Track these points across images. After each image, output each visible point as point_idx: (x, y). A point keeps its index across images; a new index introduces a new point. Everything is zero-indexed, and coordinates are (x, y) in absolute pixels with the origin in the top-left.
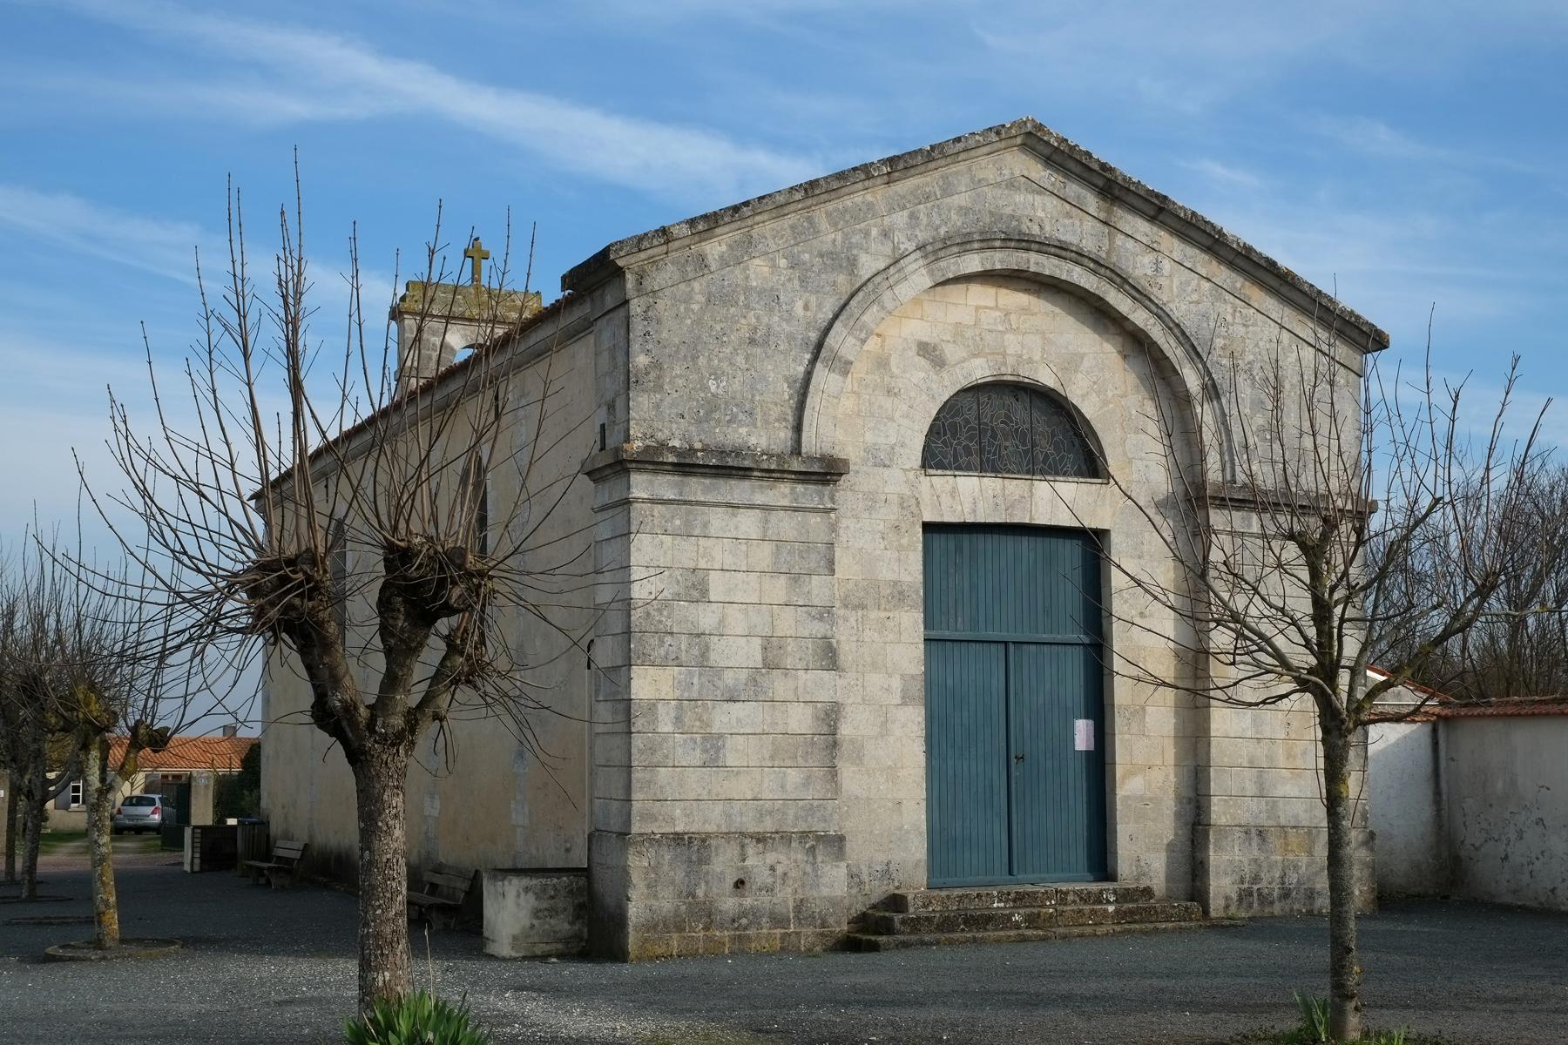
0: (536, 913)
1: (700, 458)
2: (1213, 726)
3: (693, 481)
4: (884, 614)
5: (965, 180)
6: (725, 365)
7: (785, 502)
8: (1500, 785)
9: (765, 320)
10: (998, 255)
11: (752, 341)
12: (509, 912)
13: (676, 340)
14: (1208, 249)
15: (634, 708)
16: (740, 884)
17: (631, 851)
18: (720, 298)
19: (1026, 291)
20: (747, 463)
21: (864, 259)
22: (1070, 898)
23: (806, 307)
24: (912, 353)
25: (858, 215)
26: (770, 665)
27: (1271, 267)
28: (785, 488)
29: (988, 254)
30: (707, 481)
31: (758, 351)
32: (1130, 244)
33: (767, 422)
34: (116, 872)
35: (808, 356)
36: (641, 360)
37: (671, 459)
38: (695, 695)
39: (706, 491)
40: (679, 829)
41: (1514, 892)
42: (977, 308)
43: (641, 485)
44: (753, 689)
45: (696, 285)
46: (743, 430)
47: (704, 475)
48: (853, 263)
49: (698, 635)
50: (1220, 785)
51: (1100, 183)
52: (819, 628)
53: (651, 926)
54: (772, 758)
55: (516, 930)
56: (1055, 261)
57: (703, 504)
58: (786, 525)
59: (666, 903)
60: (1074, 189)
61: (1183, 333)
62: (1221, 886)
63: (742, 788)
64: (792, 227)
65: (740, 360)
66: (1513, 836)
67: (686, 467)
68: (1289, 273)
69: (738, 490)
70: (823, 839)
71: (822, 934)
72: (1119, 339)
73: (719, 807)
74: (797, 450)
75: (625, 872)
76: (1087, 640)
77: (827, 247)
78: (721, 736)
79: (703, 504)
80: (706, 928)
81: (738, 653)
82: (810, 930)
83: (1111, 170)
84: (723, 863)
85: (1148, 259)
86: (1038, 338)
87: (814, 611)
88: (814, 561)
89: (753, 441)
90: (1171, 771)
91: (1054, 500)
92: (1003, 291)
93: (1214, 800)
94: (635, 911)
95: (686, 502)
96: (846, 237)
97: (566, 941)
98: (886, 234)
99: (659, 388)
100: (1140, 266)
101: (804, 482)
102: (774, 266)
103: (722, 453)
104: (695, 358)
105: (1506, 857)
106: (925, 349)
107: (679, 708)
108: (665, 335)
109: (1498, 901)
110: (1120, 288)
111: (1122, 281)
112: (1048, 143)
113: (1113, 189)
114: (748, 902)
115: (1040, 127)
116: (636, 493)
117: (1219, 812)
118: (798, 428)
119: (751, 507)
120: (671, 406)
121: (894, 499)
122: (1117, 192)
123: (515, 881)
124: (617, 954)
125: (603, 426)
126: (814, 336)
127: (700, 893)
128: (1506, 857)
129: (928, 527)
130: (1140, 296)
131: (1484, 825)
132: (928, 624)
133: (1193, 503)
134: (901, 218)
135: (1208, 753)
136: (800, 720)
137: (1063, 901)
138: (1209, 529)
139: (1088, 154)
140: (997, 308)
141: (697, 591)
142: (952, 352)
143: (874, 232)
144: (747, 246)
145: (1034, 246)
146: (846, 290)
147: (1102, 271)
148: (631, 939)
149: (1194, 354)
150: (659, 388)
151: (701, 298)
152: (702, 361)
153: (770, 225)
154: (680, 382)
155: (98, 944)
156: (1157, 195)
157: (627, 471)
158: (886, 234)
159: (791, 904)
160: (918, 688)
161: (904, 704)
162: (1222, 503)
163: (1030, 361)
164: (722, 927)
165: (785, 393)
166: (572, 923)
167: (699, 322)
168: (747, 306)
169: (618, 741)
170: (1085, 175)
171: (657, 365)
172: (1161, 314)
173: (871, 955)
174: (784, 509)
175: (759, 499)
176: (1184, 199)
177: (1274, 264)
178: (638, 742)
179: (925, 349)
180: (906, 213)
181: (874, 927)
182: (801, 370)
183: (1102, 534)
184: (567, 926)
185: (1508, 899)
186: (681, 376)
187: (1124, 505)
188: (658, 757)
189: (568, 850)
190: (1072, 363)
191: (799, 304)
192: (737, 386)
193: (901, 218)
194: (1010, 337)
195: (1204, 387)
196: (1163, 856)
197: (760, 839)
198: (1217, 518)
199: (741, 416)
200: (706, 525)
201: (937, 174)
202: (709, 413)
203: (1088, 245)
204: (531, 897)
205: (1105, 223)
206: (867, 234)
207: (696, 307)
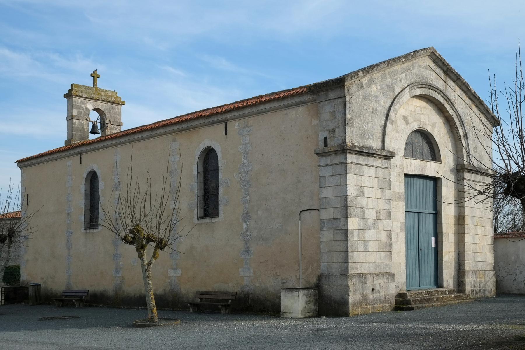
0: (306, 303)
1: (364, 150)
2: (466, 239)
3: (361, 157)
4: (397, 203)
5: (417, 65)
6: (367, 119)
7: (380, 165)
8: (513, 258)
9: (375, 106)
10: (424, 89)
11: (373, 112)
12: (296, 304)
13: (356, 111)
14: (465, 92)
15: (349, 232)
16: (373, 290)
17: (349, 279)
18: (366, 97)
19: (425, 101)
20: (374, 152)
21: (396, 88)
22: (440, 293)
23: (384, 102)
24: (402, 119)
25: (395, 73)
26: (378, 218)
27: (478, 99)
28: (380, 160)
29: (422, 89)
30: (364, 157)
31: (374, 115)
32: (450, 89)
33: (376, 139)
34: (155, 295)
35: (385, 118)
36: (348, 116)
37: (358, 150)
38: (362, 228)
39: (364, 160)
40: (359, 272)
41: (518, 290)
42: (415, 106)
43: (351, 158)
44: (374, 227)
45: (360, 93)
46: (371, 141)
47: (363, 155)
48: (394, 88)
49: (362, 208)
50: (468, 257)
51: (445, 69)
52: (387, 207)
53: (354, 305)
54: (378, 248)
55: (302, 309)
56: (435, 93)
57: (363, 165)
58: (381, 172)
59: (358, 297)
60: (439, 71)
61: (460, 118)
62: (468, 288)
63: (372, 258)
64: (381, 76)
65: (370, 118)
66: (518, 273)
67: (360, 153)
68: (482, 101)
69: (370, 161)
70: (390, 275)
71: (390, 306)
72: (443, 118)
73: (367, 265)
74: (383, 148)
75: (348, 286)
76: (434, 212)
77: (388, 83)
78: (367, 241)
79: (363, 165)
80: (366, 305)
81: (371, 214)
82: (387, 305)
83: (449, 65)
84: (369, 285)
85: (453, 94)
86: (427, 117)
87: (387, 201)
88: (386, 185)
89: (373, 145)
90: (454, 253)
91: (431, 168)
92: (420, 101)
93: (466, 262)
94: (351, 300)
95: (360, 164)
96: (392, 80)
97: (313, 312)
98: (401, 80)
99: (352, 126)
100: (452, 96)
101: (384, 159)
102: (377, 88)
103: (369, 148)
104: (360, 117)
105: (515, 280)
106: (405, 118)
107: (358, 232)
108: (354, 108)
109: (512, 293)
110: (448, 103)
111: (448, 100)
112: (436, 55)
113: (448, 72)
114: (375, 296)
115: (435, 50)
116: (349, 160)
117: (468, 266)
118: (383, 142)
119: (373, 166)
120: (356, 132)
121: (398, 165)
122: (449, 73)
123: (301, 292)
124: (345, 314)
125: (326, 139)
126: (386, 112)
127: (365, 293)
128: (515, 280)
129: (406, 175)
130: (452, 105)
131: (507, 270)
132: (406, 207)
133: (460, 169)
134: (403, 76)
135: (464, 247)
136: (384, 236)
137: (438, 294)
138: (463, 179)
139: (445, 60)
140: (419, 106)
141: (361, 194)
142: (410, 120)
143: (398, 79)
144: (371, 81)
145: (431, 88)
146: (393, 97)
147: (445, 97)
148: (350, 309)
149: (462, 124)
150: (352, 126)
151: (361, 97)
152: (362, 118)
153: (377, 75)
154: (357, 124)
155: (152, 320)
156: (458, 75)
157: (346, 153)
158: (401, 80)
159: (384, 296)
160: (404, 228)
161: (401, 232)
162: (470, 171)
163: (426, 124)
164: (370, 305)
165: (380, 130)
166: (314, 306)
167: (361, 105)
168: (371, 101)
169: (345, 242)
170: (442, 66)
171: (352, 118)
172: (456, 111)
173: (411, 311)
174: (380, 167)
175: (375, 164)
176: (464, 77)
177: (479, 98)
178: (350, 243)
179: (405, 118)
180: (405, 74)
181: (402, 303)
182: (383, 122)
183: (440, 179)
184: (313, 307)
185: (516, 292)
186: (357, 122)
187: (443, 169)
188: (354, 249)
189: (284, 283)
190: (434, 125)
191: (383, 101)
192: (369, 127)
193: (403, 76)
194: (422, 116)
195: (464, 134)
196: (452, 280)
197: (377, 275)
198: (467, 175)
199: (371, 137)
200: (364, 172)
201: (411, 62)
202: (364, 135)
203: (442, 88)
204: (305, 297)
205: (445, 82)
206: (397, 80)
207: (360, 100)
